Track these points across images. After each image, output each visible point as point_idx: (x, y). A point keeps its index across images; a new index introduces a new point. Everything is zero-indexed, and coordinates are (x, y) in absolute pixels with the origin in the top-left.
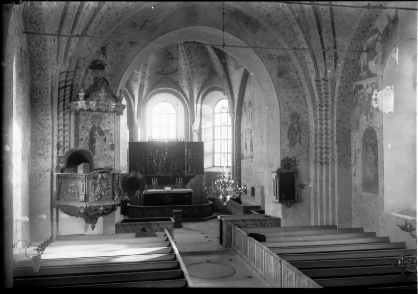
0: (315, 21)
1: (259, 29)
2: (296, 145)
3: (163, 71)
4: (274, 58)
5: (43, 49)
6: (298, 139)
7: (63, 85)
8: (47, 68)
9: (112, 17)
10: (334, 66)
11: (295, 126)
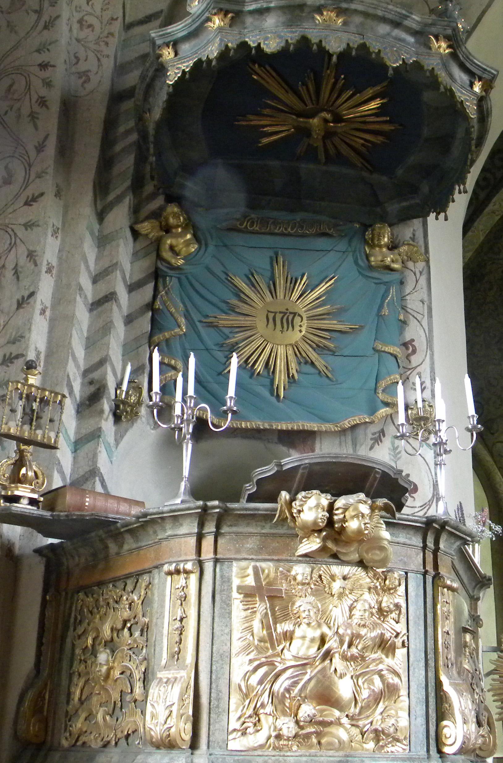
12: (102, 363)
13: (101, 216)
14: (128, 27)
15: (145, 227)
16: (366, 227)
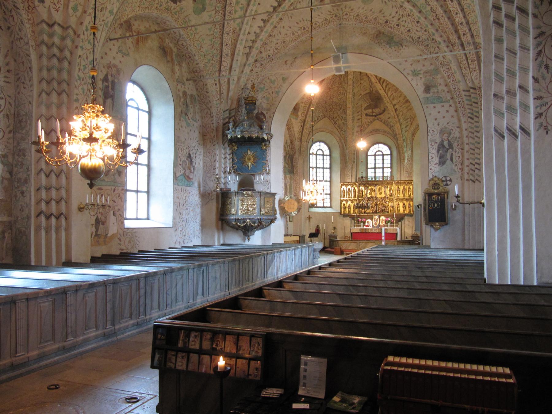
0: (450, 26)
1: (402, 47)
2: (446, 163)
3: (373, 112)
4: (420, 74)
5: (207, 92)
6: (449, 156)
7: (227, 120)
8: (211, 107)
9: (265, 59)
10: (478, 71)
11: (446, 143)
12: (226, 167)
13: (224, 145)
14: (224, 112)
15: (230, 146)
16: (261, 143)
